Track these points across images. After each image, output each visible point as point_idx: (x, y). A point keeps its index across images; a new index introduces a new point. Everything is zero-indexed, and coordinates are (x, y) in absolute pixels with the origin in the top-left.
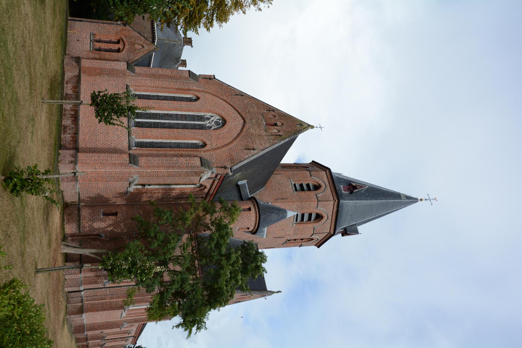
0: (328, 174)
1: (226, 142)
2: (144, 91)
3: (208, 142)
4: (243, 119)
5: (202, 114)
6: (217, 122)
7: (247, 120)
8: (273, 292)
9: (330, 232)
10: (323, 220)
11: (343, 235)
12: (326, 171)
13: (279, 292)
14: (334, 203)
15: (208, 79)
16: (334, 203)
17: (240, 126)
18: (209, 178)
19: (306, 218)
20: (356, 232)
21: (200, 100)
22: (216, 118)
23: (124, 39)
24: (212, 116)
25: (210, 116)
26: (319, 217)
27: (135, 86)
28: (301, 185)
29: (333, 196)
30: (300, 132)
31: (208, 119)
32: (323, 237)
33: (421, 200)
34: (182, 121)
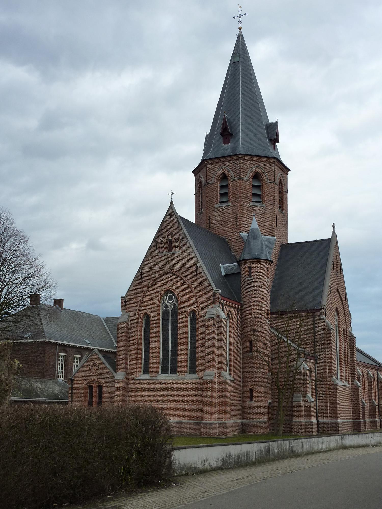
0: (210, 162)
1: (189, 292)
2: (141, 364)
3: (190, 309)
4: (166, 273)
5: (162, 312)
6: (170, 299)
7: (167, 270)
8: (334, 232)
9: (273, 163)
10: (261, 171)
11: (278, 142)
12: (206, 165)
13: (334, 227)
14: (243, 159)
15: (125, 304)
16: (243, 159)
17: (174, 277)
18: (223, 310)
19: (256, 192)
20: (275, 125)
21: (149, 312)
22: (166, 299)
23: (88, 381)
24: (164, 302)
25: (163, 304)
26: (257, 176)
27: (136, 372)
28: (222, 195)
29: (235, 160)
30: (175, 213)
31: (166, 306)
32: (279, 169)
33: (240, 29)
34: (169, 330)
